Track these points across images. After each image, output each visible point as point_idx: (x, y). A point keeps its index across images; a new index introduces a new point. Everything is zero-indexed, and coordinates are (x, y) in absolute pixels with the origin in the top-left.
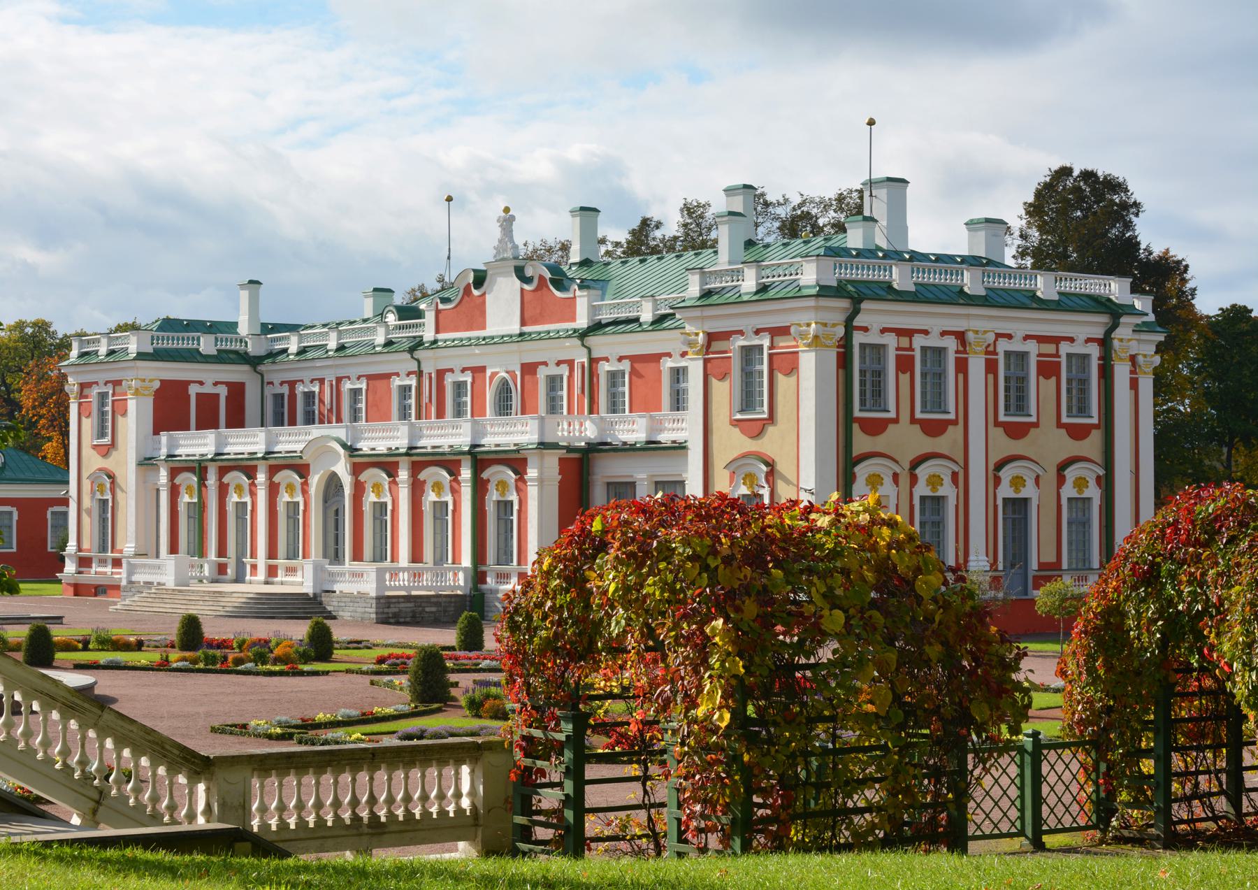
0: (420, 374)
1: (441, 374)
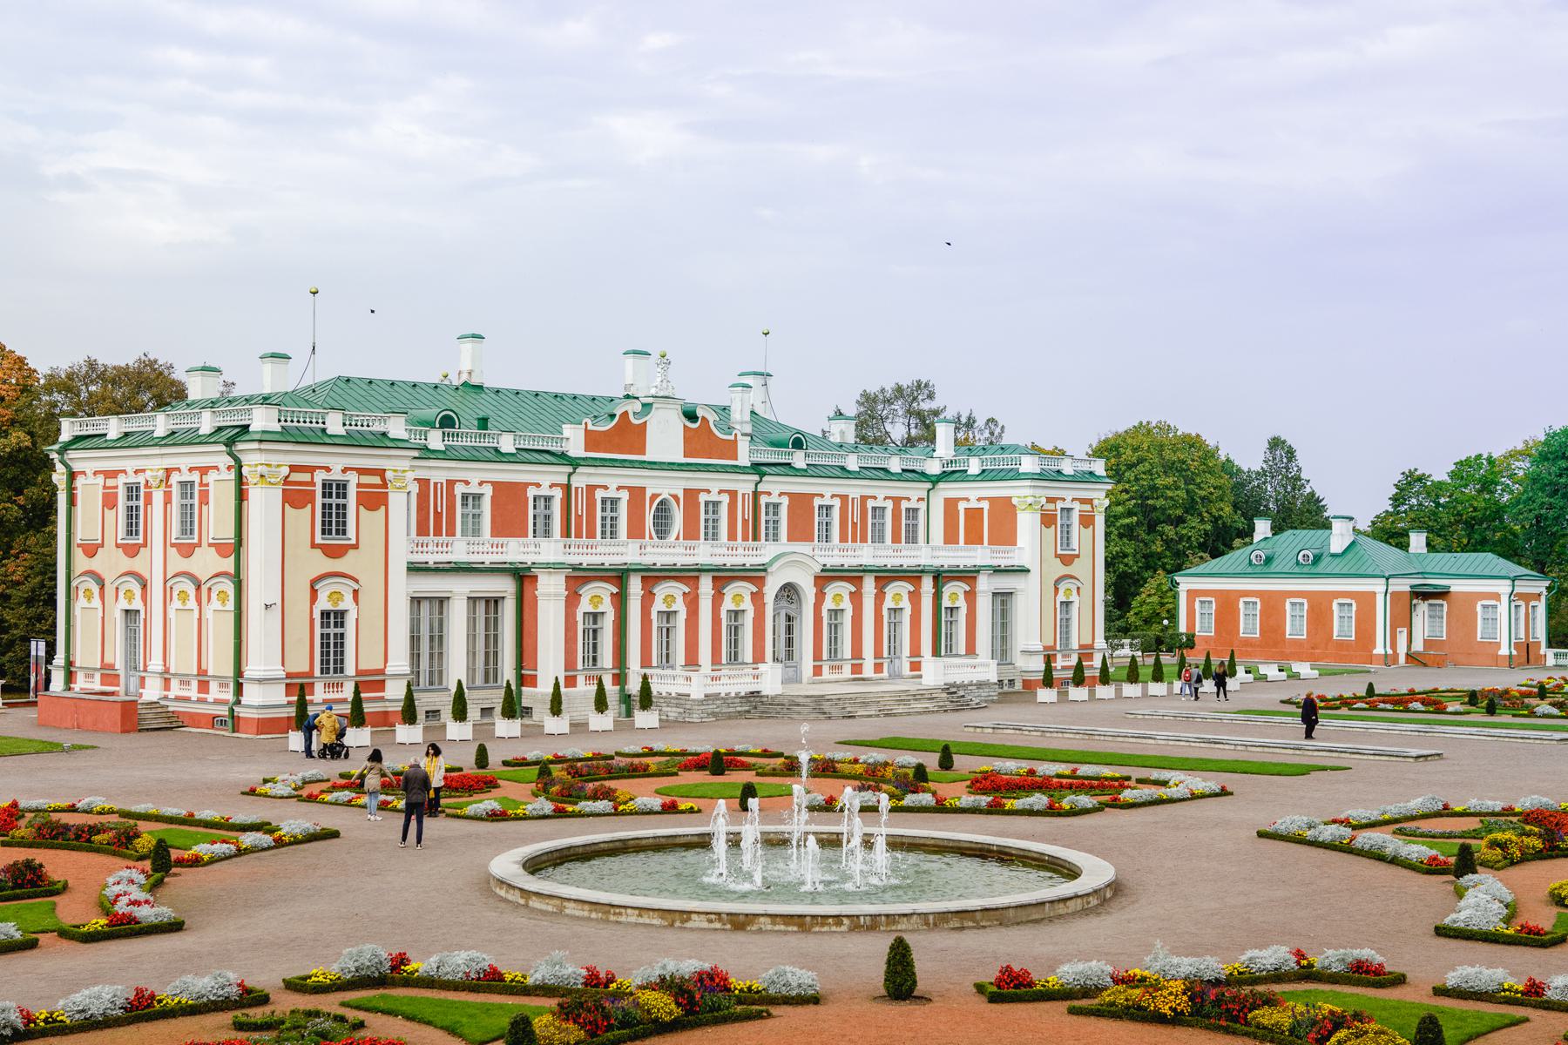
0: (567, 488)
1: (591, 489)
